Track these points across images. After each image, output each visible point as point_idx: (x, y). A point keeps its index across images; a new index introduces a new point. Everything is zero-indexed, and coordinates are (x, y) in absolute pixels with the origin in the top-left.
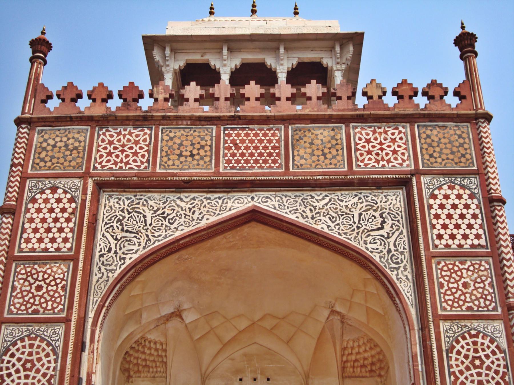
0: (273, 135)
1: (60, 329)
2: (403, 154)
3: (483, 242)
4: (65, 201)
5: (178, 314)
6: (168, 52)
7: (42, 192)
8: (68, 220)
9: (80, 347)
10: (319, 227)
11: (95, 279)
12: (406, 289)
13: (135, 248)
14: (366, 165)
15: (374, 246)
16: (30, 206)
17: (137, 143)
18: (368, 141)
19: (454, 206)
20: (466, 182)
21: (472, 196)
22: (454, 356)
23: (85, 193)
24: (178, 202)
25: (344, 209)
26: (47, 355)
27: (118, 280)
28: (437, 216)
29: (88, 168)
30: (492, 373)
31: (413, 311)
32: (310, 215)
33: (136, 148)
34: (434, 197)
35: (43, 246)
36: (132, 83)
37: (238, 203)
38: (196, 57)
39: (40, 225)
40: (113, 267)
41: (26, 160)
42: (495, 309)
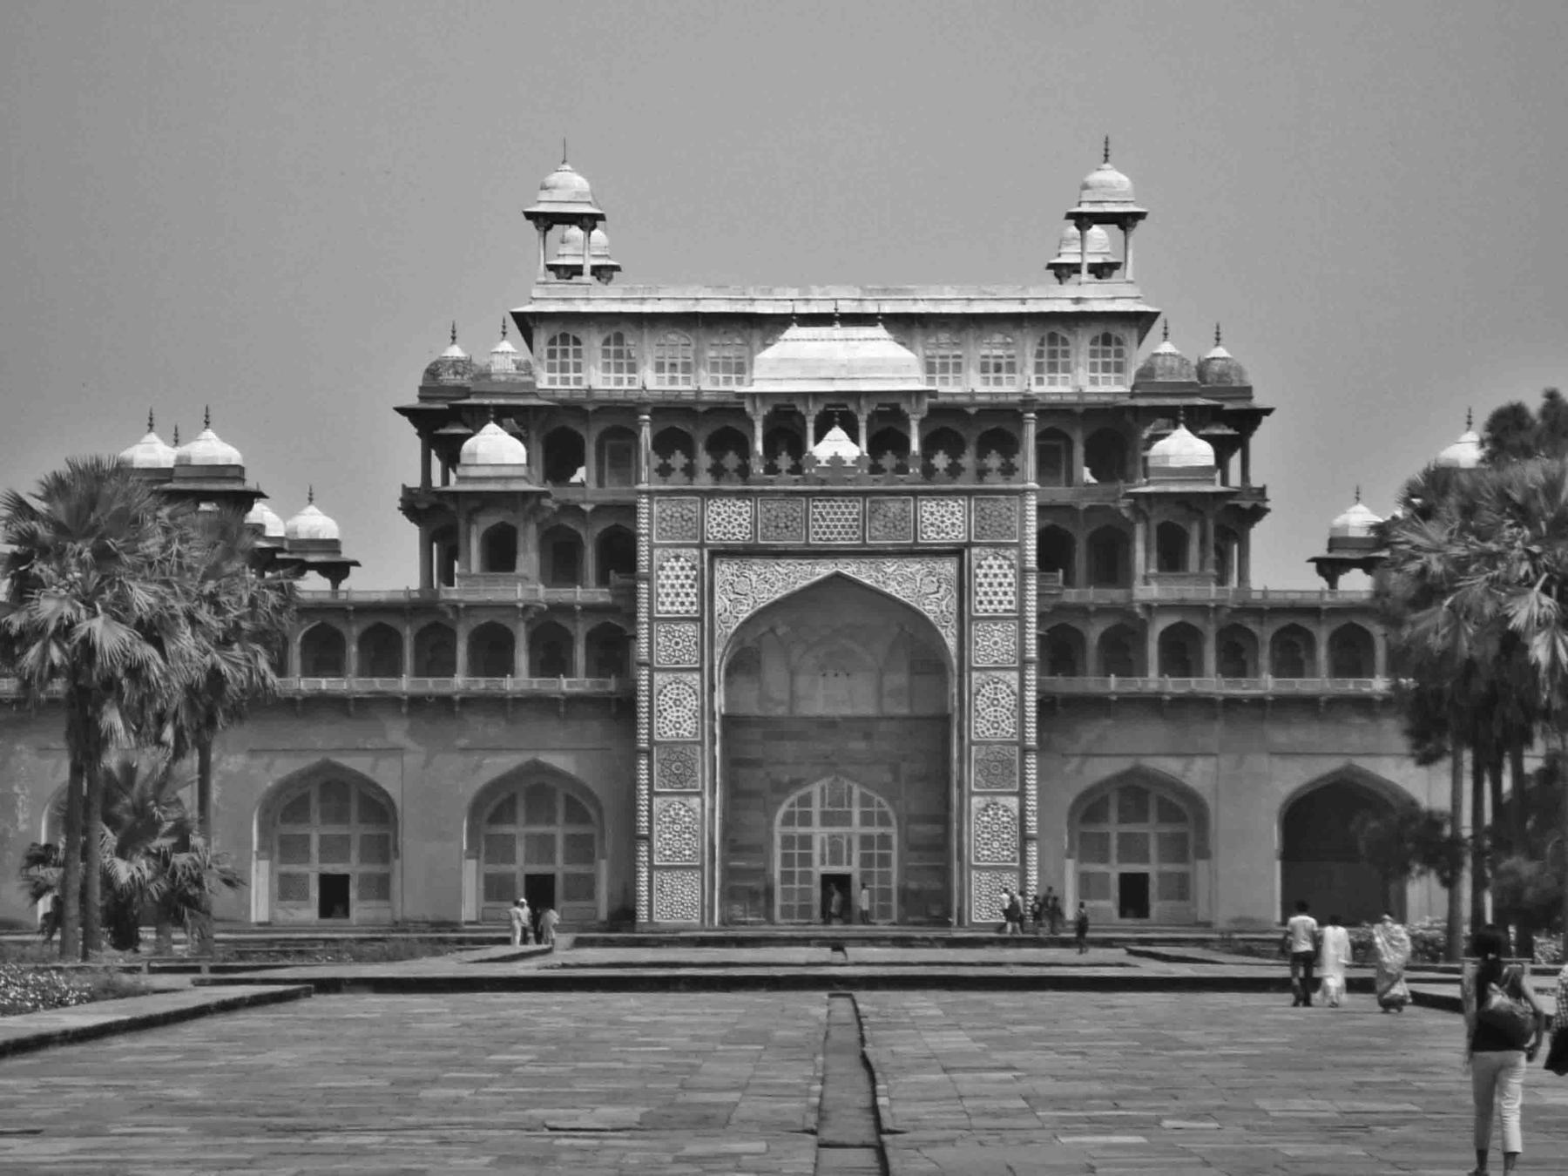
1: (697, 676)
3: (1012, 607)
5: (772, 630)
6: (758, 404)
8: (692, 586)
9: (712, 688)
10: (888, 590)
12: (951, 643)
17: (740, 514)
18: (932, 514)
19: (996, 576)
20: (1007, 553)
21: (1011, 566)
23: (702, 562)
27: (734, 634)
28: (981, 585)
31: (955, 661)
33: (740, 520)
34: (980, 566)
37: (823, 569)
38: (784, 402)
41: (650, 529)
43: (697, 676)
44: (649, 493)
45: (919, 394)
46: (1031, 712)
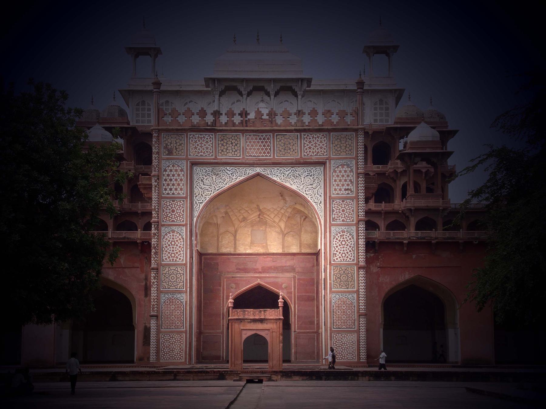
0: (268, 139)
1: (184, 228)
2: (325, 149)
4: (179, 171)
7: (169, 166)
11: (194, 207)
13: (210, 193)
14: (308, 154)
15: (309, 192)
16: (164, 173)
19: (343, 176)
21: (351, 171)
22: (335, 240)
24: (226, 171)
25: (298, 175)
26: (180, 239)
29: (187, 155)
30: (348, 247)
32: (282, 177)
35: (172, 192)
36: (202, 108)
37: (251, 172)
39: (170, 182)
40: (201, 201)
42: (353, 221)
43: (184, 228)
44: (159, 131)
45: (302, 80)
46: (362, 248)
